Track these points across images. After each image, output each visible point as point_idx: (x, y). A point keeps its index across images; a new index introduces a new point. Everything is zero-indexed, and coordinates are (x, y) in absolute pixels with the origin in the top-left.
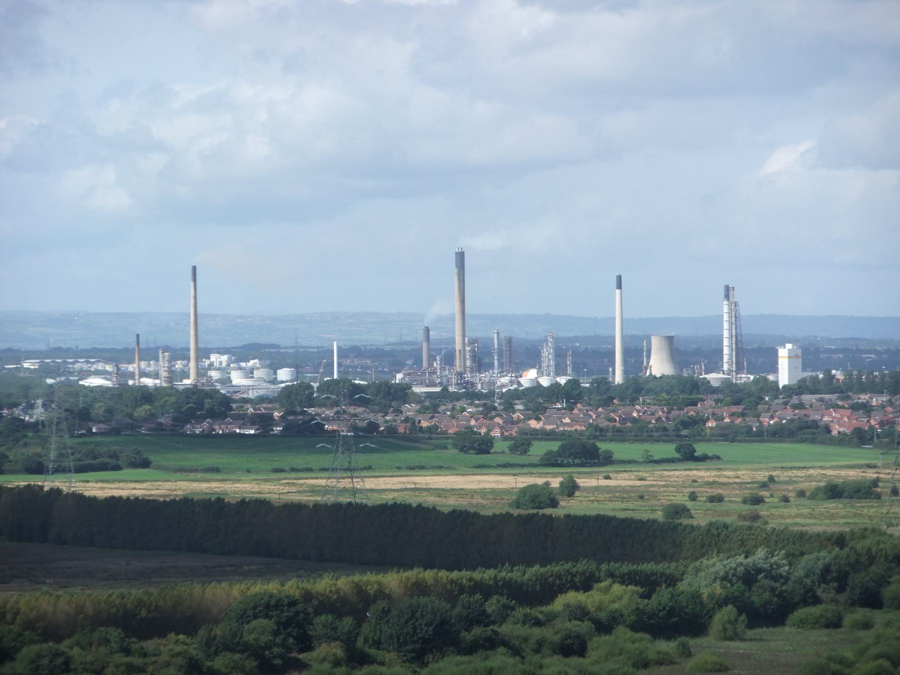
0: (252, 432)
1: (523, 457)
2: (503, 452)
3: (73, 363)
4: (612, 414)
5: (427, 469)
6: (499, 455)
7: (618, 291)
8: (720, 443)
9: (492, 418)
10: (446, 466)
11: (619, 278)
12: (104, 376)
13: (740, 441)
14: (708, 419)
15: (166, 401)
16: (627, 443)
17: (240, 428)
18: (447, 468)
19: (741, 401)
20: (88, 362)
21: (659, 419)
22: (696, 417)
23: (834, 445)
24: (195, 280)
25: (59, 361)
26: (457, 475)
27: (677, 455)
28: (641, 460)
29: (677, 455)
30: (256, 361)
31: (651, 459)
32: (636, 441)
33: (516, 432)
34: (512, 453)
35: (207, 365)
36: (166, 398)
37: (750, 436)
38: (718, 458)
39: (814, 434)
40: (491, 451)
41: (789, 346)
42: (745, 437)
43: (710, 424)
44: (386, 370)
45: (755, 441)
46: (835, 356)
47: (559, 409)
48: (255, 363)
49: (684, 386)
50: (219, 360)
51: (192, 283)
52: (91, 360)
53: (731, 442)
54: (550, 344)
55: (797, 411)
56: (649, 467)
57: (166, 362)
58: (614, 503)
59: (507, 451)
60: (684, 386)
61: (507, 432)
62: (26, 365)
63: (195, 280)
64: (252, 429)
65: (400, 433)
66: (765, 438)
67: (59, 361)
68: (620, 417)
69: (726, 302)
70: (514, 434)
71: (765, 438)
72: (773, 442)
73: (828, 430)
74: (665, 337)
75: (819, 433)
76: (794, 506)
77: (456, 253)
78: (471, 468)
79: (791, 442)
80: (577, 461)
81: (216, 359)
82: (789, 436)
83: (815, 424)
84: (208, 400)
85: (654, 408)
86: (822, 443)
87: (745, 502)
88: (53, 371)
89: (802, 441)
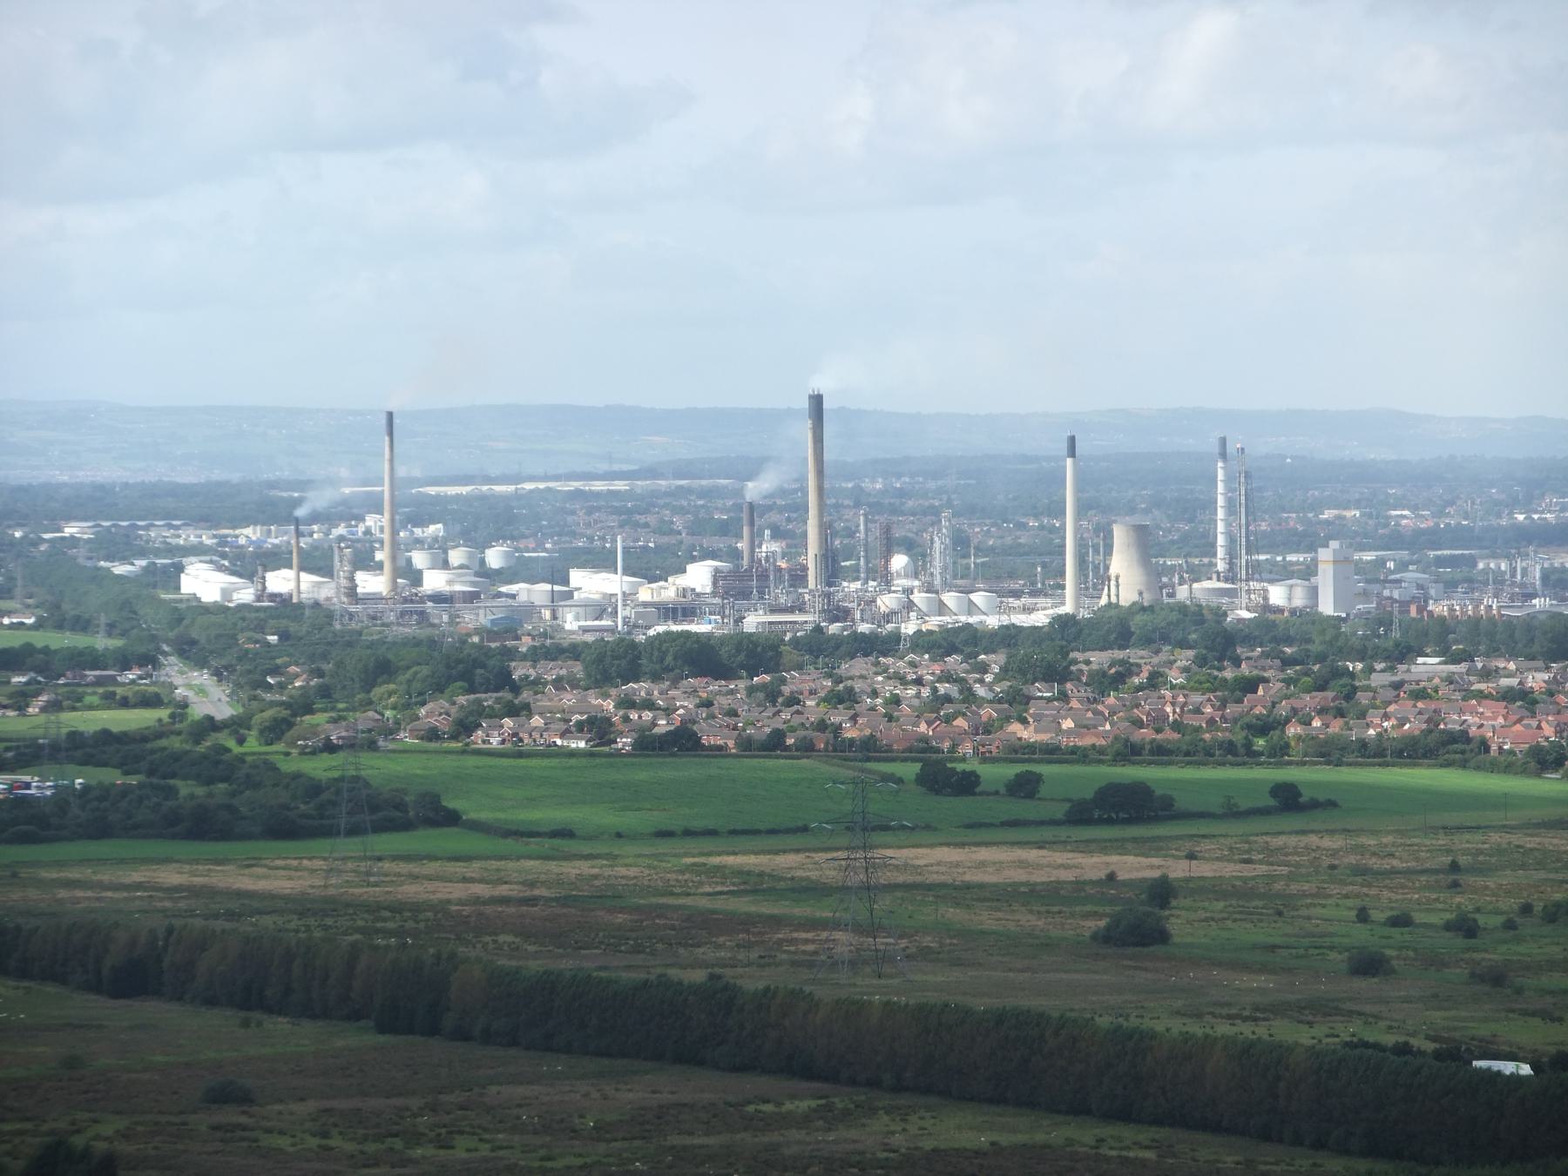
0: (582, 744)
1: (1029, 803)
2: (997, 793)
3: (146, 528)
4: (1135, 711)
5: (894, 830)
6: (991, 798)
7: (1069, 461)
8: (1319, 767)
9: (948, 720)
10: (923, 825)
11: (1072, 440)
12: (208, 558)
13: (1349, 764)
14: (1287, 721)
15: (416, 673)
16: (1174, 767)
17: (562, 736)
18: (924, 828)
19: (1327, 682)
20: (170, 526)
21: (1211, 722)
22: (1268, 716)
23: (1499, 772)
24: (391, 434)
25: (124, 524)
26: (948, 845)
27: (1272, 802)
28: (1219, 811)
29: (1272, 802)
30: (440, 526)
31: (1235, 809)
32: (1189, 763)
33: (998, 747)
34: (1011, 795)
35: (360, 534)
36: (414, 669)
37: (1363, 756)
38: (1332, 804)
39: (1463, 752)
40: (978, 790)
41: (1334, 544)
42: (1357, 757)
43: (1293, 730)
44: (651, 545)
45: (1374, 765)
46: (1349, 514)
47: (1049, 700)
48: (439, 530)
49: (1213, 641)
50: (379, 524)
51: (387, 439)
52: (174, 523)
53: (1337, 765)
54: (944, 530)
55: (1420, 705)
56: (1237, 828)
57: (346, 563)
58: (1239, 923)
59: (1003, 790)
60: (1213, 641)
61: (983, 746)
62: (296, 685)
63: (391, 434)
64: (582, 739)
65: (819, 751)
66: (1389, 759)
67: (124, 524)
68: (1148, 714)
69: (1220, 464)
70: (994, 750)
71: (1389, 759)
72: (1401, 765)
73: (1484, 746)
74: (1134, 526)
75: (1472, 751)
76: (1528, 938)
77: (811, 397)
78: (959, 827)
79: (1429, 766)
80: (1121, 815)
81: (375, 522)
82: (1425, 756)
83: (1463, 737)
84: (479, 671)
85: (1197, 698)
86: (1478, 768)
87: (1448, 927)
88: (123, 547)
89: (1449, 764)
